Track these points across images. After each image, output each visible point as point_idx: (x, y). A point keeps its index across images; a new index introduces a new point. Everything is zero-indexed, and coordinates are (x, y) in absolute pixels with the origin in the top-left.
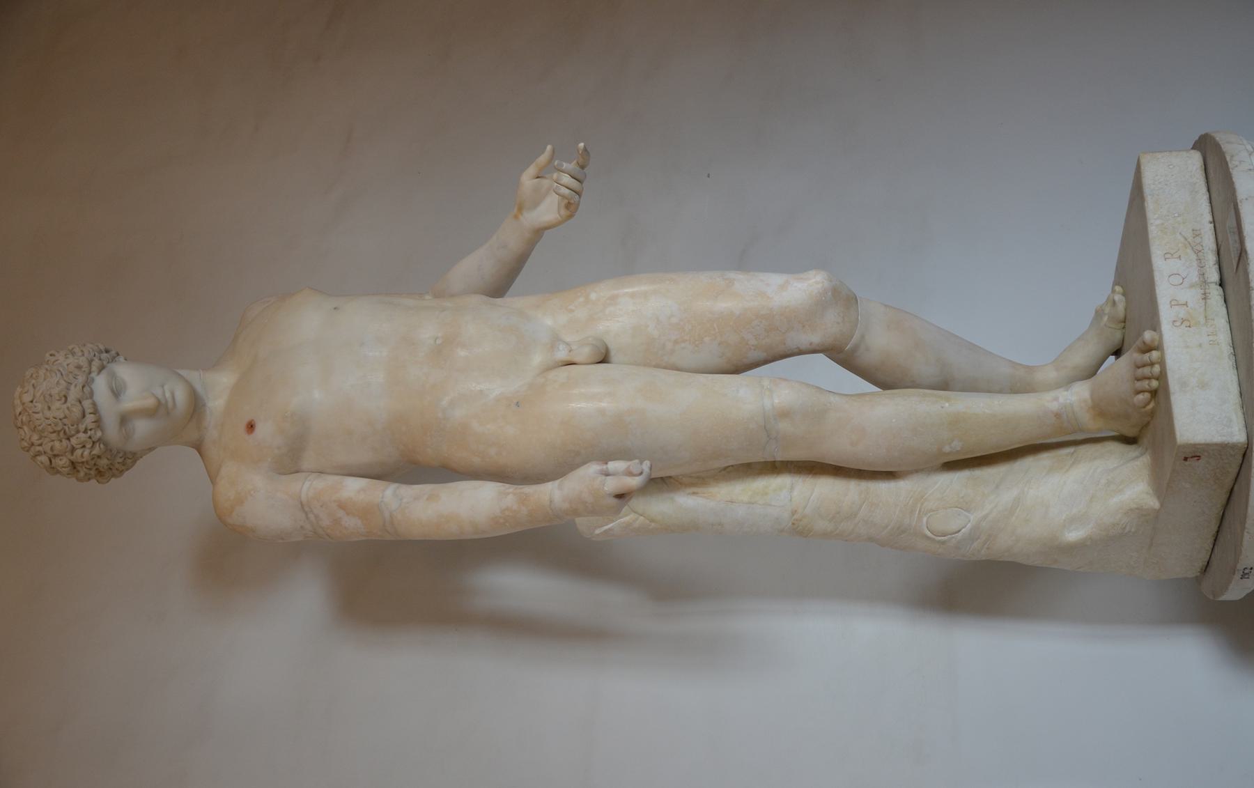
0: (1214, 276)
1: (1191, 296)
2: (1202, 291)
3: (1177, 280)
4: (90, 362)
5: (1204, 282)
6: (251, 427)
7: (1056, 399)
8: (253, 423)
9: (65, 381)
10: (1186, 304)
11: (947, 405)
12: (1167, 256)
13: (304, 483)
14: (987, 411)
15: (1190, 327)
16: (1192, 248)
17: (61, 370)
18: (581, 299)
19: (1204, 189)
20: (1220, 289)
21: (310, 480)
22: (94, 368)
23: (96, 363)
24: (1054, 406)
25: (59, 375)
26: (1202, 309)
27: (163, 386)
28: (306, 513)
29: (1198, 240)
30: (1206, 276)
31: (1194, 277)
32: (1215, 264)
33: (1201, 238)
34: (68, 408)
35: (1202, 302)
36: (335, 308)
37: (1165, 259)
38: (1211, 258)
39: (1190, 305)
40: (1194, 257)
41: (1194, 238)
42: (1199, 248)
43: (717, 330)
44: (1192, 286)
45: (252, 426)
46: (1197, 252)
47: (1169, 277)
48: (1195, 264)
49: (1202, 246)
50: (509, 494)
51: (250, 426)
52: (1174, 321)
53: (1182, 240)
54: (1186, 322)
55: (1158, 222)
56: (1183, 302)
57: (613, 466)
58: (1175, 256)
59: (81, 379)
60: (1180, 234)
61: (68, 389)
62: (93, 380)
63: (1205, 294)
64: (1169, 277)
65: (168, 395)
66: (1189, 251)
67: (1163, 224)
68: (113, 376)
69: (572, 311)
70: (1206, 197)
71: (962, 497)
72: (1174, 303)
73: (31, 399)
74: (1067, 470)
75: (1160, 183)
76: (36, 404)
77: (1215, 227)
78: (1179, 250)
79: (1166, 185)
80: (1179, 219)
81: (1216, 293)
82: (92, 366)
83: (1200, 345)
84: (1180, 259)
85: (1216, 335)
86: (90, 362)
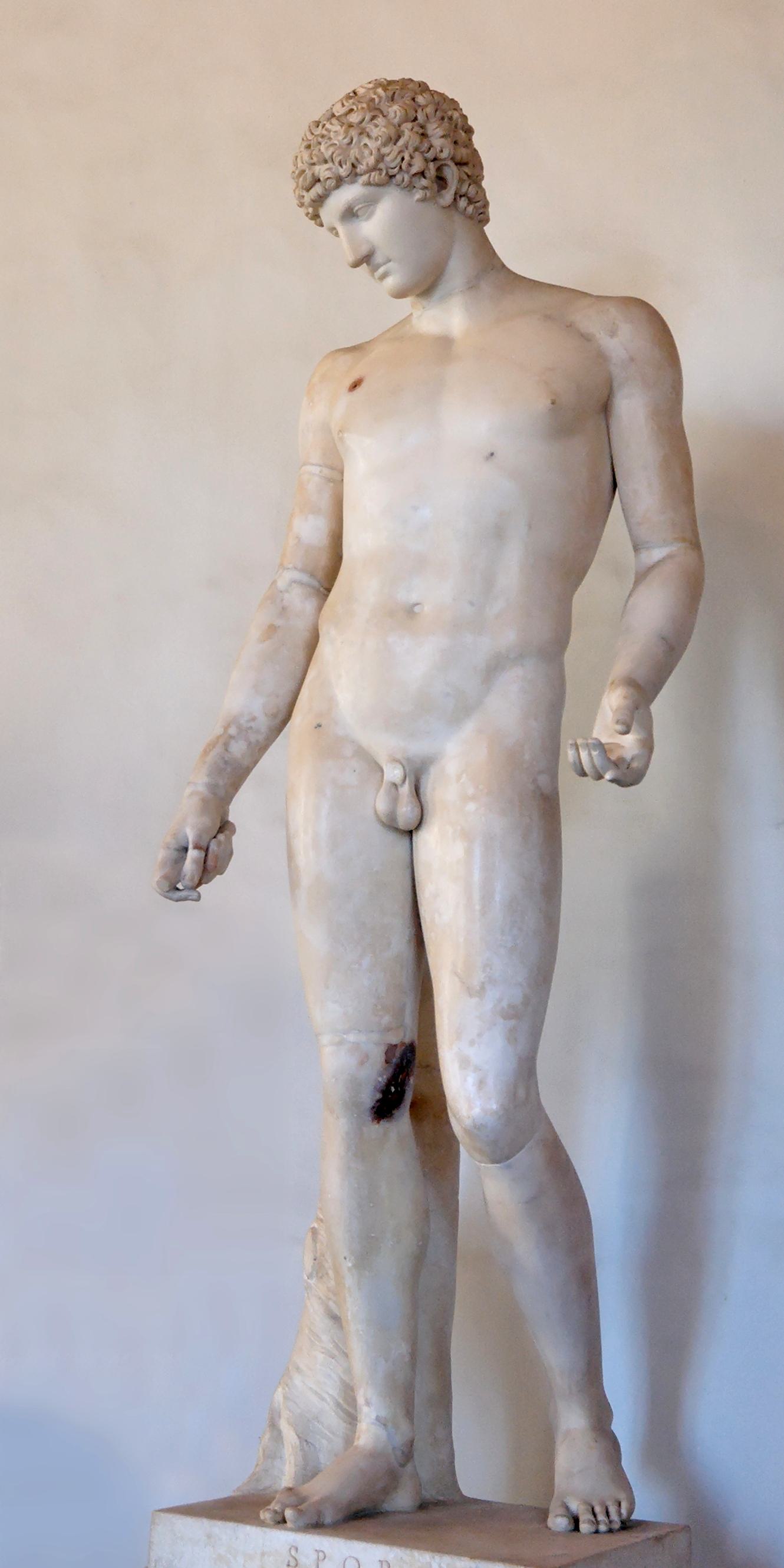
4: (375, 169)
7: (368, 1403)
9: (333, 153)
11: (350, 1265)
14: (349, 1314)
15: (288, 1565)
17: (354, 142)
18: (471, 791)
22: (365, 178)
23: (375, 176)
25: (346, 141)
45: (356, 386)
52: (297, 1549)
57: (192, 854)
59: (343, 171)
61: (326, 162)
62: (353, 182)
68: (371, 202)
72: (321, 1556)
74: (338, 1405)
76: (320, 127)
82: (367, 175)
86: (375, 169)
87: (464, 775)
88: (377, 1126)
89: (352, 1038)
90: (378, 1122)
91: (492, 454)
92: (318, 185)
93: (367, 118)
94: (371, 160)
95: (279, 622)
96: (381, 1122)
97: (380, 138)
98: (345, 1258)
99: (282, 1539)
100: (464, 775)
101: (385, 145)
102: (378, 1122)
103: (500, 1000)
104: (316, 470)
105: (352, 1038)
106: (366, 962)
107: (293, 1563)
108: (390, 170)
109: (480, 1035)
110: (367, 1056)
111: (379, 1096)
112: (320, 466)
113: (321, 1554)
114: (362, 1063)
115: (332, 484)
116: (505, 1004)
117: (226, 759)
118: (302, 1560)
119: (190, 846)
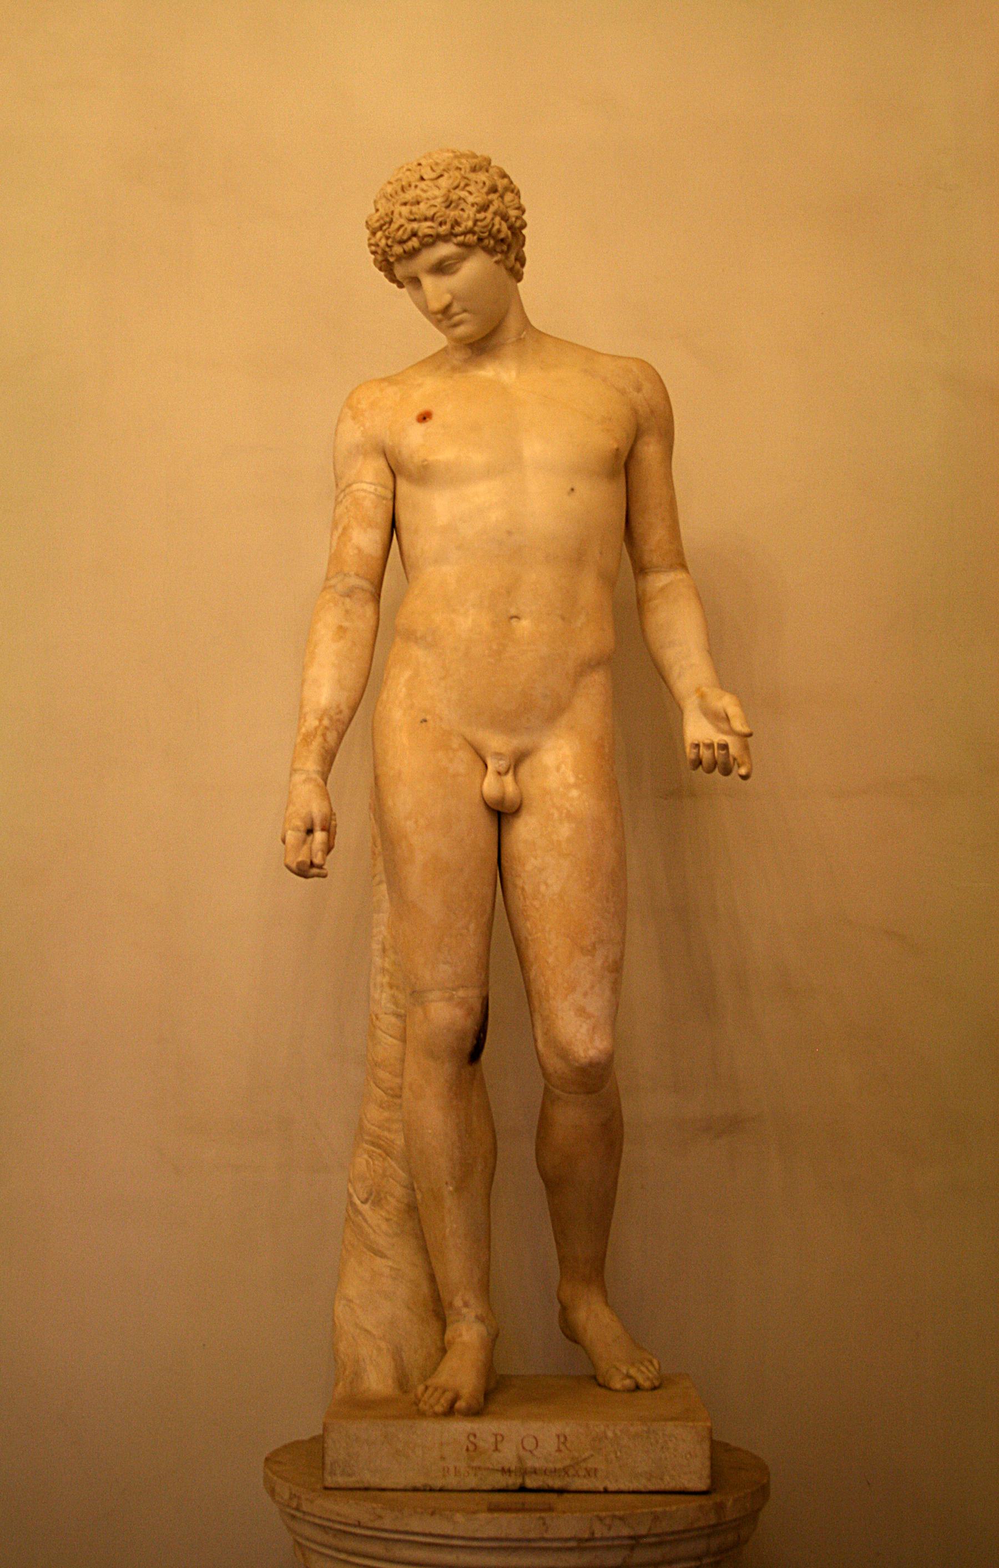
0: (530, 1483)
1: (508, 1455)
2: (513, 1468)
3: (529, 1444)
4: (471, 231)
5: (524, 1472)
6: (424, 417)
7: (466, 1305)
8: (427, 419)
10: (496, 1449)
11: (451, 1188)
12: (563, 1439)
13: (371, 483)
14: (448, 1230)
16: (570, 1466)
19: (651, 1487)
20: (517, 1486)
21: (376, 490)
22: (461, 238)
24: (458, 1302)
26: (488, 1465)
27: (465, 311)
28: (344, 490)
29: (582, 1473)
30: (534, 1475)
31: (531, 1463)
32: (548, 1486)
33: (585, 1476)
34: (401, 226)
35: (499, 1467)
36: (572, 490)
37: (558, 1436)
38: (557, 1483)
39: (496, 1455)
40: (559, 1466)
41: (586, 1469)
42: (571, 1472)
43: (536, 936)
44: (520, 1459)
45: (424, 419)
46: (565, 1471)
47: (535, 1438)
48: (551, 1466)
49: (574, 1476)
50: (320, 720)
51: (422, 417)
52: (475, 1436)
53: (583, 1457)
54: (473, 1449)
55: (610, 1434)
56: (499, 1446)
58: (562, 1447)
60: (592, 1456)
63: (509, 1471)
64: (535, 1438)
65: (457, 318)
66: (568, 1462)
67: (606, 1437)
68: (461, 259)
69: (558, 769)
70: (642, 1488)
71: (386, 1198)
72: (499, 1439)
73: (425, 177)
75: (666, 1442)
77: (599, 1492)
78: (570, 1451)
79: (662, 1448)
80: (613, 1456)
81: (512, 1481)
83: (443, 1458)
84: (557, 1451)
85: (455, 1475)
87: (563, 766)
88: (470, 1068)
89: (461, 993)
90: (472, 1065)
91: (572, 490)
92: (414, 239)
93: (462, 185)
94: (470, 224)
95: (346, 624)
96: (473, 1064)
97: (476, 206)
98: (447, 1183)
99: (459, 1428)
100: (563, 766)
101: (479, 212)
102: (472, 1065)
103: (607, 957)
104: (372, 488)
105: (461, 993)
106: (472, 927)
107: (471, 1448)
108: (481, 234)
109: (592, 987)
110: (472, 1009)
111: (475, 1042)
112: (374, 485)
113: (499, 1438)
114: (469, 1014)
115: (384, 502)
116: (610, 960)
117: (326, 748)
118: (481, 1444)
119: (317, 828)
